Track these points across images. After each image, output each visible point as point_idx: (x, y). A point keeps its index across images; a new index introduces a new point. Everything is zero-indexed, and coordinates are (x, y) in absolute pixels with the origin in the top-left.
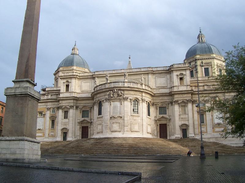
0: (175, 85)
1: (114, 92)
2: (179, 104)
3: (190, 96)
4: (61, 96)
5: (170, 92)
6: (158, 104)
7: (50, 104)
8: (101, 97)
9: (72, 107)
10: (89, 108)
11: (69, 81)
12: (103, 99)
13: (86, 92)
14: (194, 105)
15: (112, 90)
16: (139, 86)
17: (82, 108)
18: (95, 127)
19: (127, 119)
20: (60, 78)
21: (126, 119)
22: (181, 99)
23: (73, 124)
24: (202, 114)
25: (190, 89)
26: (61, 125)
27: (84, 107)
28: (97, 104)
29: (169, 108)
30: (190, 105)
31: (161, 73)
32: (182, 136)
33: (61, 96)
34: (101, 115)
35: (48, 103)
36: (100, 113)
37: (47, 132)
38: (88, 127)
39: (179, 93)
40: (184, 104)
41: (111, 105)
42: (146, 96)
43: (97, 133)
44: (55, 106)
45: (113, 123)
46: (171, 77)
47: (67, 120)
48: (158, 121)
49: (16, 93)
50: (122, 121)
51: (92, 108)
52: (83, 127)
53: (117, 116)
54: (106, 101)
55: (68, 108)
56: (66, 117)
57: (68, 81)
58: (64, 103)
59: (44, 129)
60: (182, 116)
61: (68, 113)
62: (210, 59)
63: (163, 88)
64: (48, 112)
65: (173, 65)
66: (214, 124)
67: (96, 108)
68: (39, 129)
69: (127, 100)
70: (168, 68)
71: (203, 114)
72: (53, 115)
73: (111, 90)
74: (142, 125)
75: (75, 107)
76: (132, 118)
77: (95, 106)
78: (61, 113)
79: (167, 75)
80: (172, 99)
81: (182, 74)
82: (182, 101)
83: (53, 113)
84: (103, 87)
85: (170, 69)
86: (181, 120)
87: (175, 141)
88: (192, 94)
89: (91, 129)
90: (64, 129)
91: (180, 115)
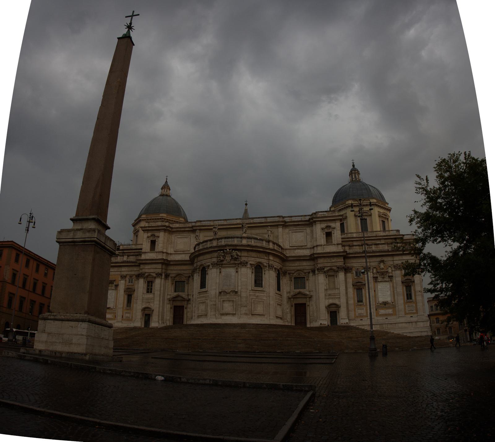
0: (318, 244)
1: (227, 253)
2: (325, 272)
3: (342, 260)
4: (143, 257)
5: (311, 254)
6: (293, 274)
8: (206, 260)
9: (159, 275)
10: (186, 277)
11: (157, 234)
12: (209, 264)
13: (182, 252)
14: (347, 274)
15: (223, 250)
16: (264, 244)
17: (175, 277)
18: (195, 306)
19: (245, 295)
20: (143, 230)
21: (244, 294)
22: (328, 265)
23: (160, 301)
24: (359, 287)
25: (342, 250)
27: (178, 275)
28: (199, 270)
29: (310, 279)
30: (341, 275)
31: (298, 225)
32: (329, 324)
33: (143, 257)
34: (205, 288)
35: (123, 268)
36: (203, 285)
37: (120, 313)
38: (184, 306)
39: (325, 255)
40: (331, 273)
41: (220, 272)
42: (275, 260)
43: (198, 316)
44: (133, 273)
45: (224, 301)
46: (312, 231)
47: (151, 295)
48: (292, 299)
49: (75, 240)
50: (237, 298)
51: (190, 277)
52: (175, 307)
53: (230, 290)
54: (213, 267)
56: (149, 290)
57: (153, 235)
58: (147, 269)
60: (330, 292)
64: (123, 282)
65: (315, 213)
66: (378, 304)
67: (197, 278)
69: (245, 266)
70: (307, 218)
71: (361, 289)
72: (130, 286)
73: (221, 250)
74: (268, 305)
75: (163, 275)
76: (253, 294)
77: (195, 275)
78: (141, 285)
79: (306, 228)
80: (314, 265)
82: (328, 268)
84: (209, 245)
85: (312, 219)
86: (327, 297)
87: (321, 329)
89: (188, 310)
90: (147, 309)
91: (326, 290)
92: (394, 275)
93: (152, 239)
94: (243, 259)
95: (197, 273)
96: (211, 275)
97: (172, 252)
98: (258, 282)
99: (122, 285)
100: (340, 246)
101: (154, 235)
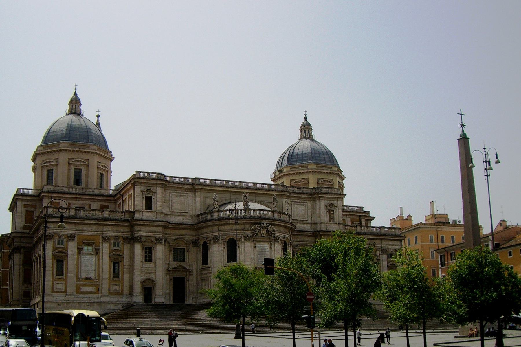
7: (110, 228)
8: (238, 232)
9: (158, 240)
12: (239, 237)
13: (179, 214)
15: (260, 224)
26: (139, 273)
31: (300, 197)
33: (137, 216)
35: (104, 227)
37: (105, 285)
41: (255, 247)
44: (119, 234)
46: (313, 207)
55: (152, 242)
56: (148, 257)
58: (143, 232)
59: (99, 277)
61: (153, 252)
62: (332, 175)
63: (302, 222)
64: (106, 245)
68: (87, 279)
73: (257, 223)
81: (331, 205)
83: (115, 248)
92: (381, 259)
93: (146, 194)
95: (219, 243)
96: (244, 249)
97: (167, 213)
99: (105, 248)
100: (341, 226)
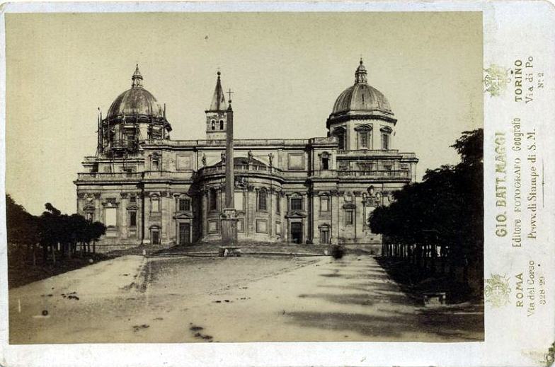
2: (319, 196)
37: (124, 231)
75: (168, 194)
81: (326, 153)
88: (338, 183)
94: (250, 184)
98: (262, 206)
101: (157, 154)
